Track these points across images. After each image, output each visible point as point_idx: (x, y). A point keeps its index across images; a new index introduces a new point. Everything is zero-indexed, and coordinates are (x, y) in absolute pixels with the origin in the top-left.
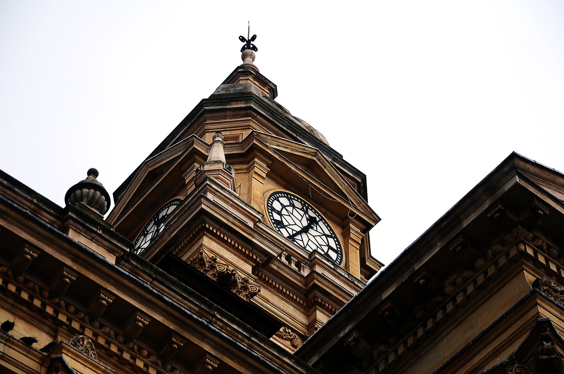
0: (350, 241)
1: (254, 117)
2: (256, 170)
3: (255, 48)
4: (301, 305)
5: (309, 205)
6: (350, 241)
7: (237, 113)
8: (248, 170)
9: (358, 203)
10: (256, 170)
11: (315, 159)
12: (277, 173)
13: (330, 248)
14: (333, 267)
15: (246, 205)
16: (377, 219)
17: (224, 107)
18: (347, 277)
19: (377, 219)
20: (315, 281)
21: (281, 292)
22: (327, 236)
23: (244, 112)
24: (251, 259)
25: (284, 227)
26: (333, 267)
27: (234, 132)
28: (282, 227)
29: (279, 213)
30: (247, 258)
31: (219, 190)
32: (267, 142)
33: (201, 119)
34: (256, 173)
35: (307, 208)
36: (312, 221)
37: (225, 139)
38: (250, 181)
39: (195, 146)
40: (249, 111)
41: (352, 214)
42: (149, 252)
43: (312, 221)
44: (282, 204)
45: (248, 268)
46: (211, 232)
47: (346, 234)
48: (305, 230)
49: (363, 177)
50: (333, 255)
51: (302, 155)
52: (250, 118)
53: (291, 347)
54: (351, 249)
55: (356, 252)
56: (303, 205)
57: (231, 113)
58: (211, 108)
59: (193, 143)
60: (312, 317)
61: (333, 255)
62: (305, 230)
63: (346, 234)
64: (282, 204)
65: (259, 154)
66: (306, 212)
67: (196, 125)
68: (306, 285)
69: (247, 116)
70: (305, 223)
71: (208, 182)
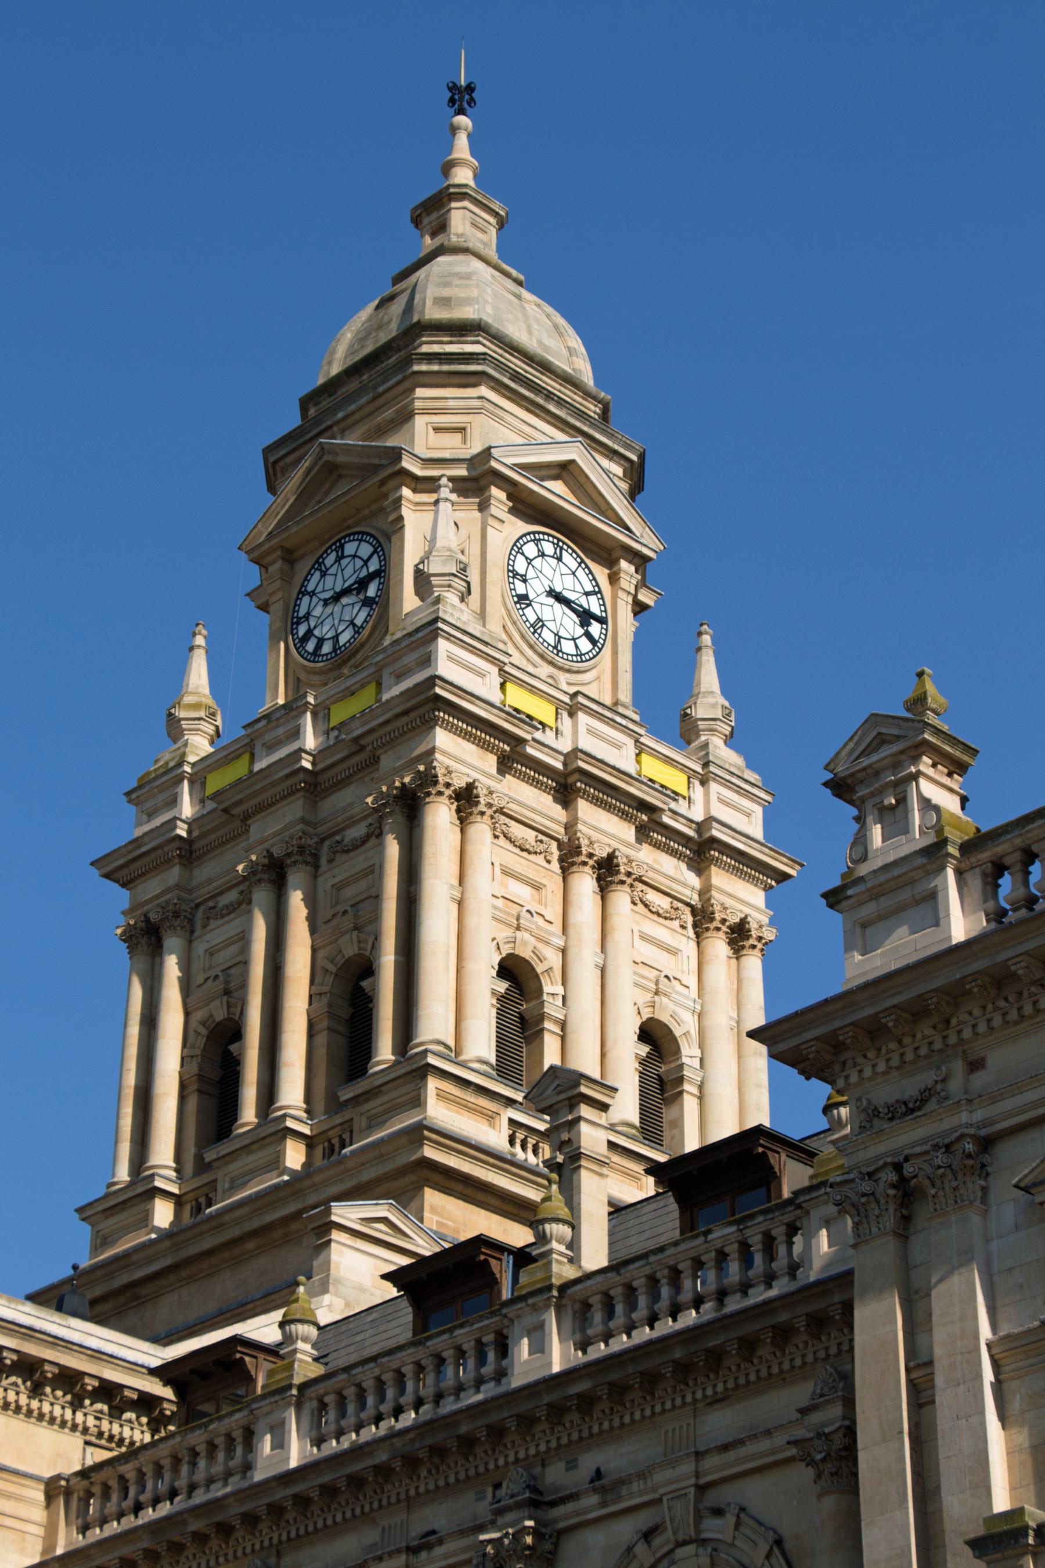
2: (493, 510)
5: (564, 543)
8: (483, 507)
34: (492, 515)
35: (561, 549)
44: (527, 558)
54: (621, 604)
63: (613, 579)
64: (527, 558)
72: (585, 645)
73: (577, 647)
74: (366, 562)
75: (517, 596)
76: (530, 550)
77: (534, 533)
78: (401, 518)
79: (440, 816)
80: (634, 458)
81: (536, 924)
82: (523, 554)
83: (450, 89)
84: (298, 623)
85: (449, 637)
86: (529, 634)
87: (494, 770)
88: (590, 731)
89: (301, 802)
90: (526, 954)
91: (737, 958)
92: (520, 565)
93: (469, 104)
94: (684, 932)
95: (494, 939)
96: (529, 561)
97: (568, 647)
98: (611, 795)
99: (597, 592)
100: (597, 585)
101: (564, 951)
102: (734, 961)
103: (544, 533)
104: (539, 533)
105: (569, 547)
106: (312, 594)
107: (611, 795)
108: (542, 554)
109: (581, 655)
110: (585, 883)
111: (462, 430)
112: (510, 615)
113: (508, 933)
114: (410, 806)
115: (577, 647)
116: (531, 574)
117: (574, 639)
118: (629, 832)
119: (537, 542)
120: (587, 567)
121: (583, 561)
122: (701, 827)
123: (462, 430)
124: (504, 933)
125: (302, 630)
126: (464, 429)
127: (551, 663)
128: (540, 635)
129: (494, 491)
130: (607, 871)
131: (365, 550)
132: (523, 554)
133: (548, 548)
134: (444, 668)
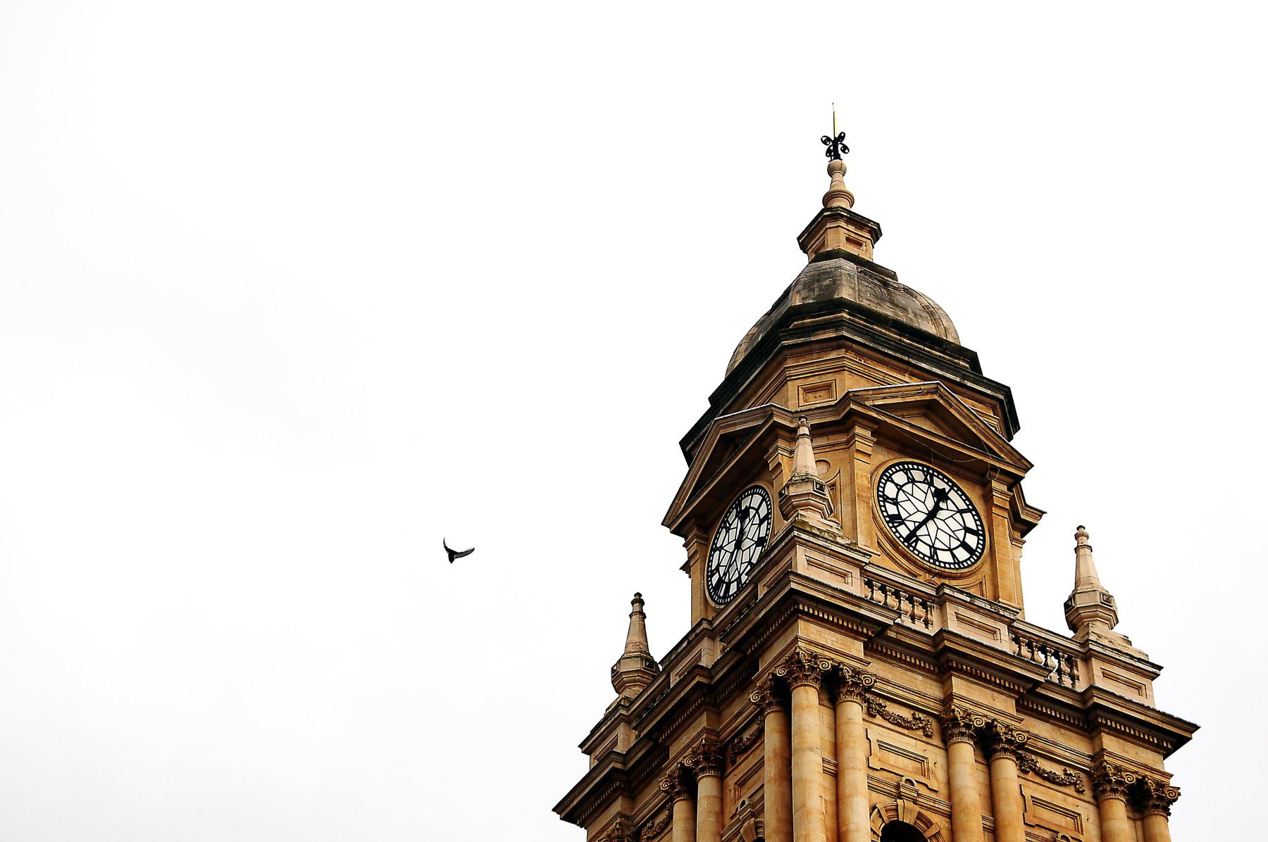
0: (994, 510)
1: (848, 349)
2: (859, 446)
3: (845, 148)
4: (932, 672)
6: (994, 510)
7: (824, 345)
8: (849, 443)
9: (1000, 449)
10: (859, 446)
11: (936, 397)
12: (887, 437)
13: (967, 530)
14: (968, 599)
15: (847, 548)
16: (1027, 466)
17: (808, 339)
18: (988, 607)
19: (1027, 466)
20: (947, 643)
21: (905, 662)
22: (961, 512)
23: (835, 343)
24: (862, 634)
25: (902, 523)
26: (968, 599)
27: (825, 378)
28: (900, 524)
29: (895, 502)
30: (855, 634)
31: (811, 539)
32: (868, 399)
33: (780, 358)
34: (858, 451)
35: (932, 476)
36: (941, 496)
37: (814, 428)
38: (851, 463)
39: (775, 419)
40: (841, 342)
41: (995, 469)
42: (735, 632)
43: (941, 496)
44: (896, 485)
45: (857, 648)
46: (807, 614)
47: (987, 498)
48: (932, 515)
49: (1006, 391)
50: (972, 540)
51: (918, 398)
52: (842, 353)
53: (924, 739)
54: (997, 521)
55: (1003, 524)
56: (926, 473)
57: (817, 346)
58: (791, 342)
59: (772, 415)
60: (947, 685)
61: (972, 540)
62: (932, 515)
63: (987, 498)
64: (896, 485)
65: (859, 420)
66: (931, 484)
67: (774, 365)
68: (935, 646)
69: (839, 347)
70: (930, 503)
71: (796, 533)
72: (962, 554)
73: (954, 556)
74: (757, 510)
75: (889, 516)
76: (900, 478)
77: (903, 464)
78: (779, 464)
79: (807, 699)
80: (1001, 397)
81: (916, 791)
82: (892, 481)
83: (825, 143)
84: (712, 575)
85: (806, 544)
86: (903, 546)
87: (862, 656)
88: (960, 618)
89: (704, 717)
90: (909, 819)
91: (1142, 819)
92: (890, 490)
93: (843, 151)
94: (1082, 797)
95: (874, 808)
96: (900, 488)
97: (945, 557)
98: (984, 669)
99: (971, 509)
100: (971, 504)
101: (950, 816)
102: (1139, 823)
103: (913, 463)
104: (908, 463)
105: (939, 473)
106: (721, 547)
107: (984, 669)
108: (912, 481)
109: (959, 563)
110: (966, 752)
111: (827, 387)
112: (881, 530)
113: (889, 801)
114: (781, 696)
115: (954, 556)
116: (902, 497)
117: (950, 550)
118: (1006, 704)
119: (906, 471)
120: (959, 489)
121: (954, 485)
122: (1085, 696)
123: (827, 387)
124: (883, 801)
125: (715, 579)
126: (830, 385)
127: (929, 571)
128: (915, 548)
129: (858, 430)
130: (988, 743)
131: (757, 499)
132: (892, 481)
133: (918, 475)
134: (802, 568)
